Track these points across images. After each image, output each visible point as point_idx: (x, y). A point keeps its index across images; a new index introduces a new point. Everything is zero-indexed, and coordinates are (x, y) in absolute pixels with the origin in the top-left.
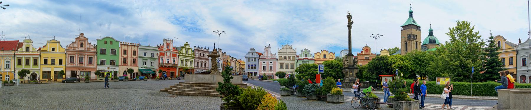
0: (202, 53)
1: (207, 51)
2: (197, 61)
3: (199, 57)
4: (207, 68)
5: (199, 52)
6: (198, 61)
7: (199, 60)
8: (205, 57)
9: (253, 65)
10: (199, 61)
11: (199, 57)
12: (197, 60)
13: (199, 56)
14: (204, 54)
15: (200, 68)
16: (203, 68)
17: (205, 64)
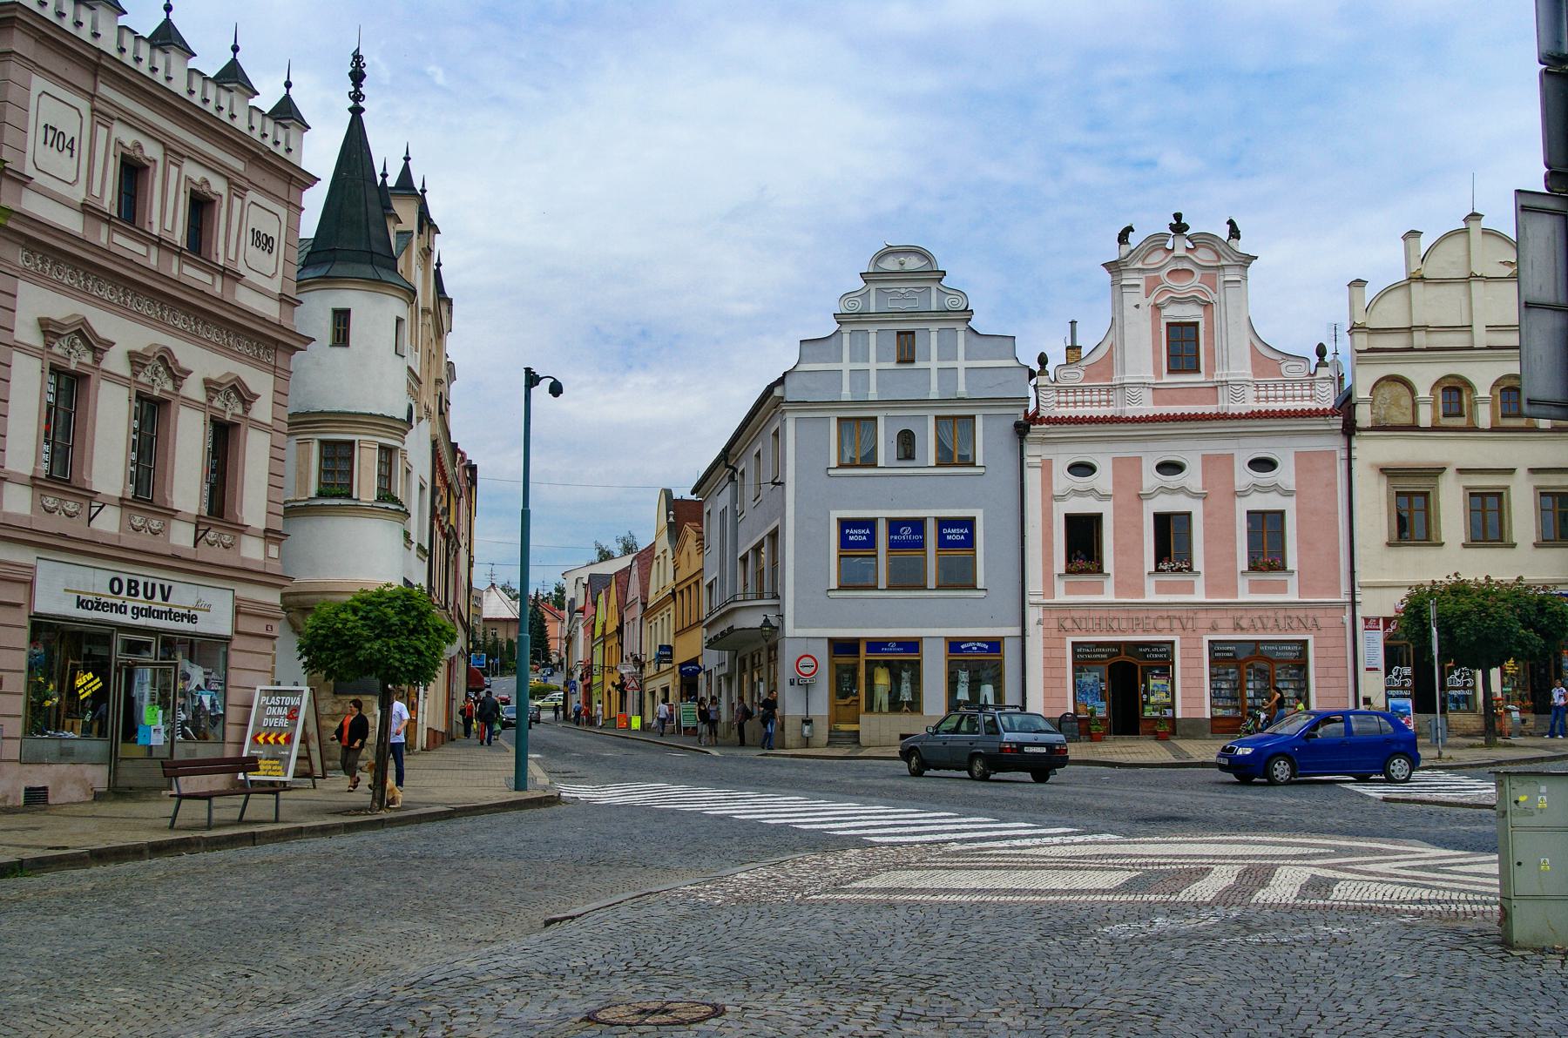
0: (175, 153)
1: (271, 136)
2: (49, 329)
3: (103, 236)
4: (252, 551)
5: (102, 116)
6: (83, 333)
7: (104, 323)
8: (231, 276)
9: (918, 525)
10: (98, 347)
11: (103, 236)
12: (62, 307)
13: (88, 210)
14: (200, 205)
15: (108, 522)
16: (181, 536)
17: (223, 437)
